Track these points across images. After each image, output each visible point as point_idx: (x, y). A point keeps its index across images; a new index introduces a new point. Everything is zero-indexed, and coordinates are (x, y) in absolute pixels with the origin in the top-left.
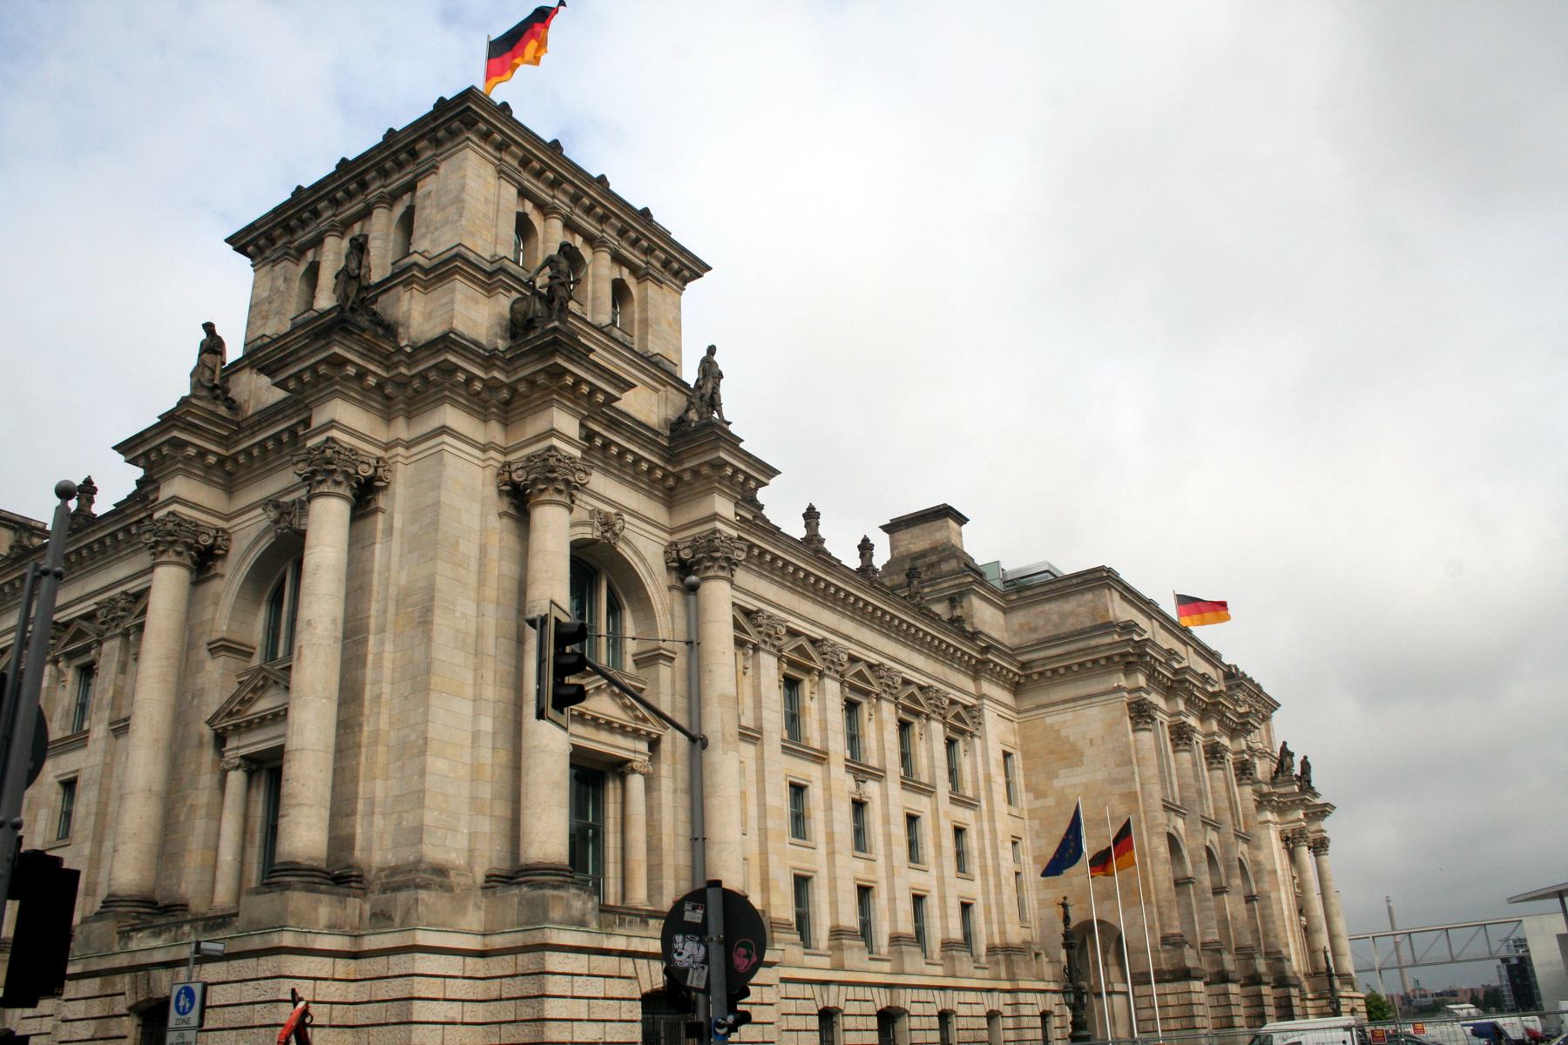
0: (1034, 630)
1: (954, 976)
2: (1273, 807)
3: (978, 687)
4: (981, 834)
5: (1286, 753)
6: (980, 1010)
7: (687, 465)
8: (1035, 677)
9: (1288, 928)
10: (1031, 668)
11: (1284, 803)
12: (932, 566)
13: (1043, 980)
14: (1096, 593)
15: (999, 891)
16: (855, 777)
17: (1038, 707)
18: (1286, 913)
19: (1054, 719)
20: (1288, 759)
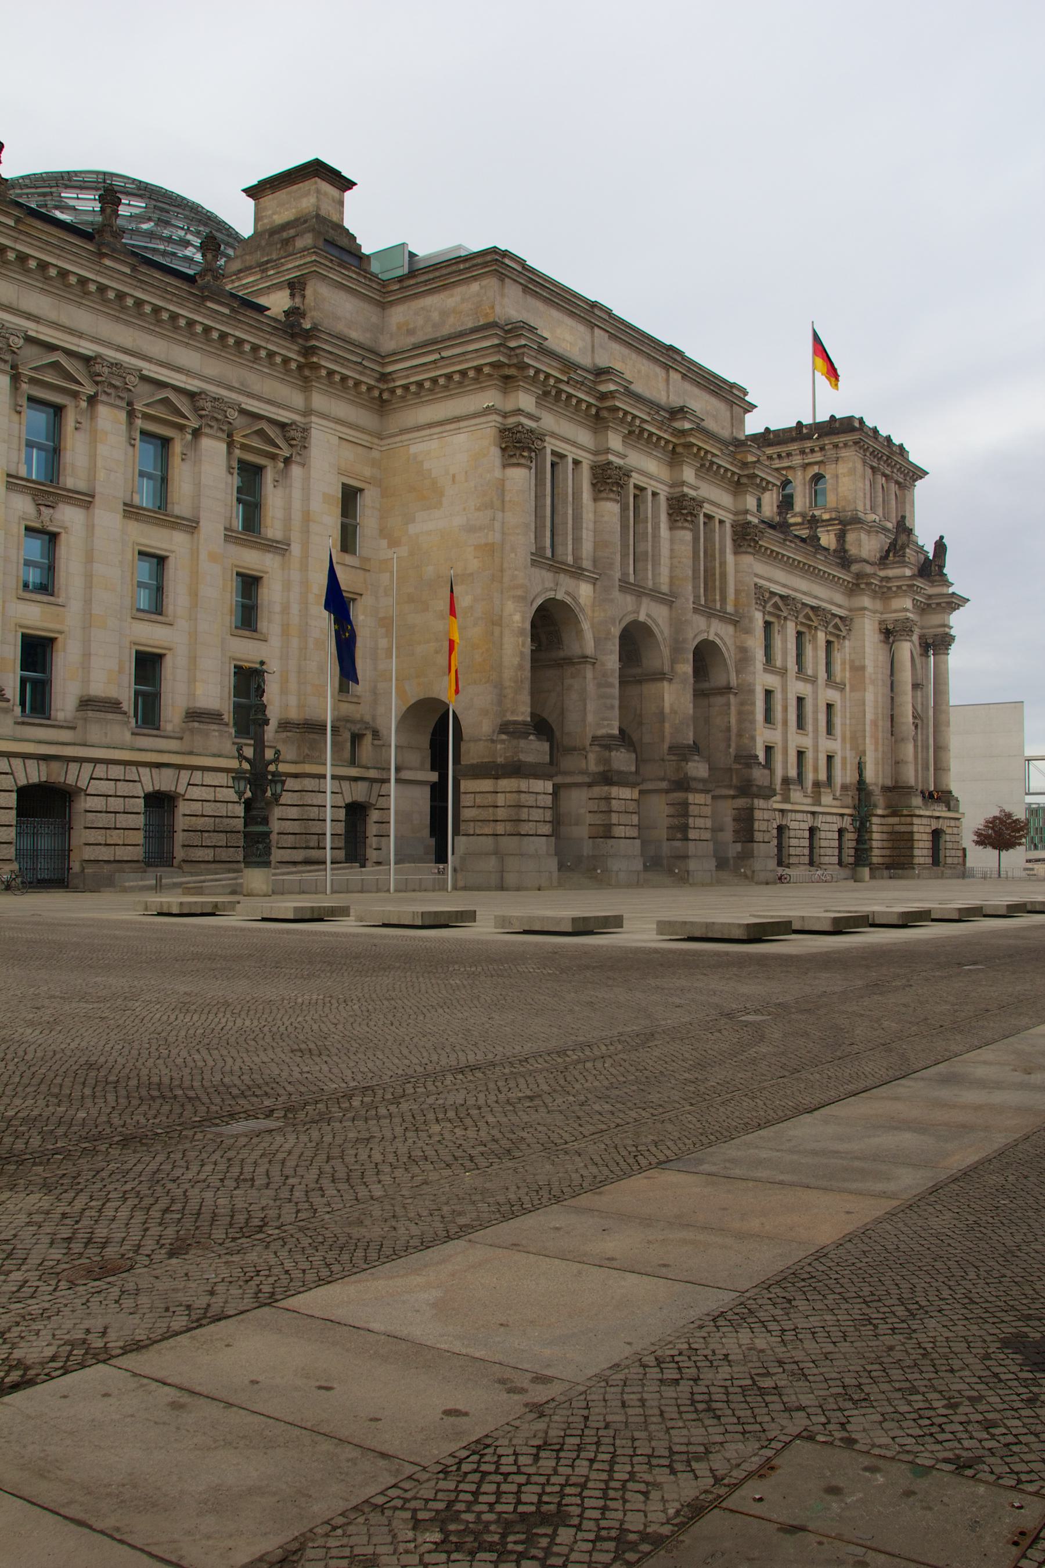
0: (411, 332)
1: (191, 753)
2: (874, 591)
4: (287, 586)
8: (399, 392)
9: (868, 734)
10: (394, 380)
11: (889, 588)
12: (286, 242)
14: (484, 282)
16: (34, 500)
17: (403, 431)
18: (869, 716)
20: (903, 538)
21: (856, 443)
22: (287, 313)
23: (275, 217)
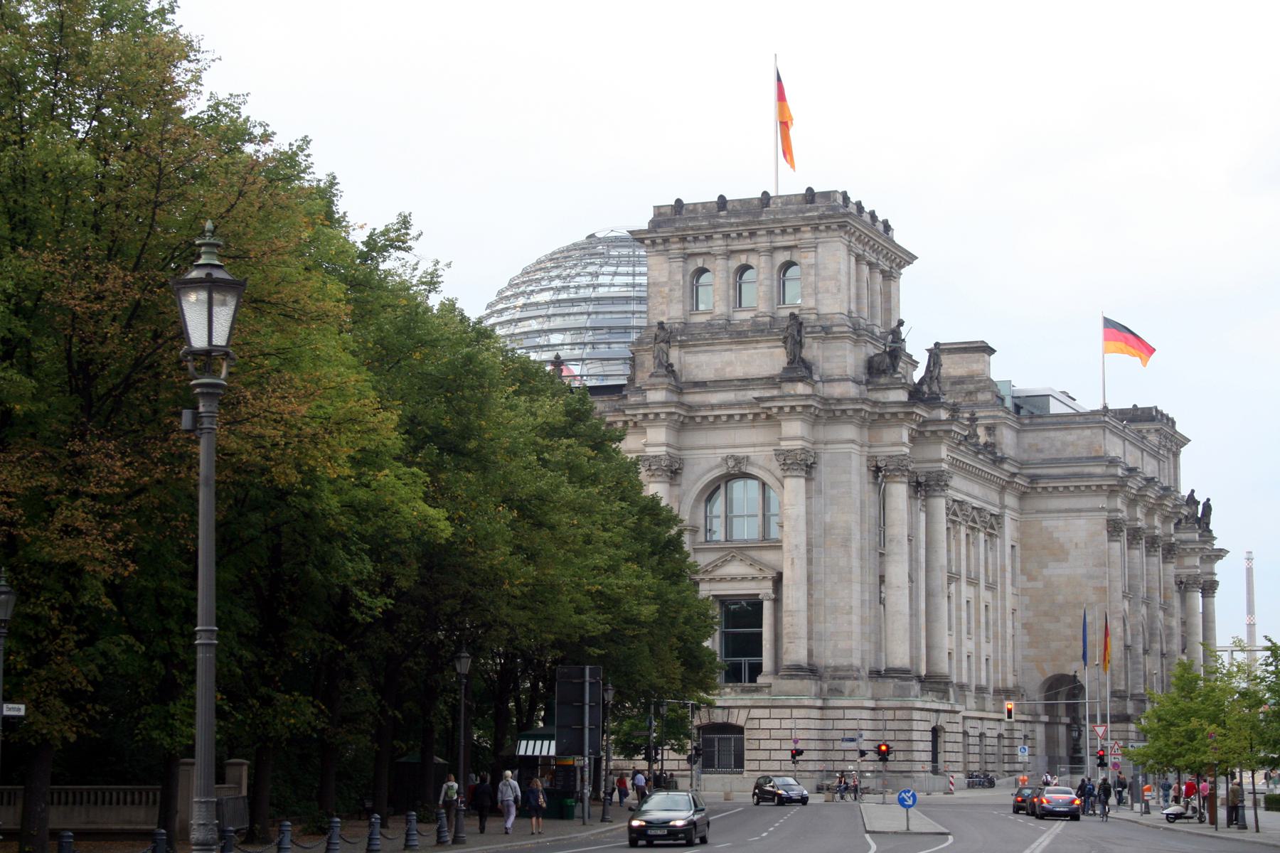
3: (1002, 499)
4: (996, 609)
5: (1191, 500)
6: (995, 734)
7: (929, 428)
8: (1039, 490)
11: (1184, 549)
12: (970, 393)
13: (1023, 713)
14: (1095, 431)
15: (1004, 651)
17: (1038, 512)
19: (1050, 523)
21: (1157, 430)
22: (986, 445)
23: (951, 370)
